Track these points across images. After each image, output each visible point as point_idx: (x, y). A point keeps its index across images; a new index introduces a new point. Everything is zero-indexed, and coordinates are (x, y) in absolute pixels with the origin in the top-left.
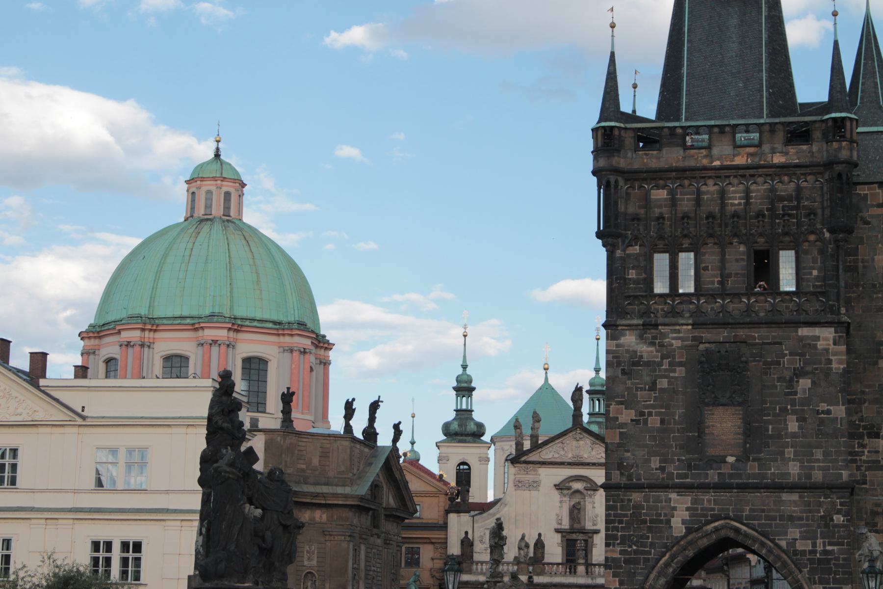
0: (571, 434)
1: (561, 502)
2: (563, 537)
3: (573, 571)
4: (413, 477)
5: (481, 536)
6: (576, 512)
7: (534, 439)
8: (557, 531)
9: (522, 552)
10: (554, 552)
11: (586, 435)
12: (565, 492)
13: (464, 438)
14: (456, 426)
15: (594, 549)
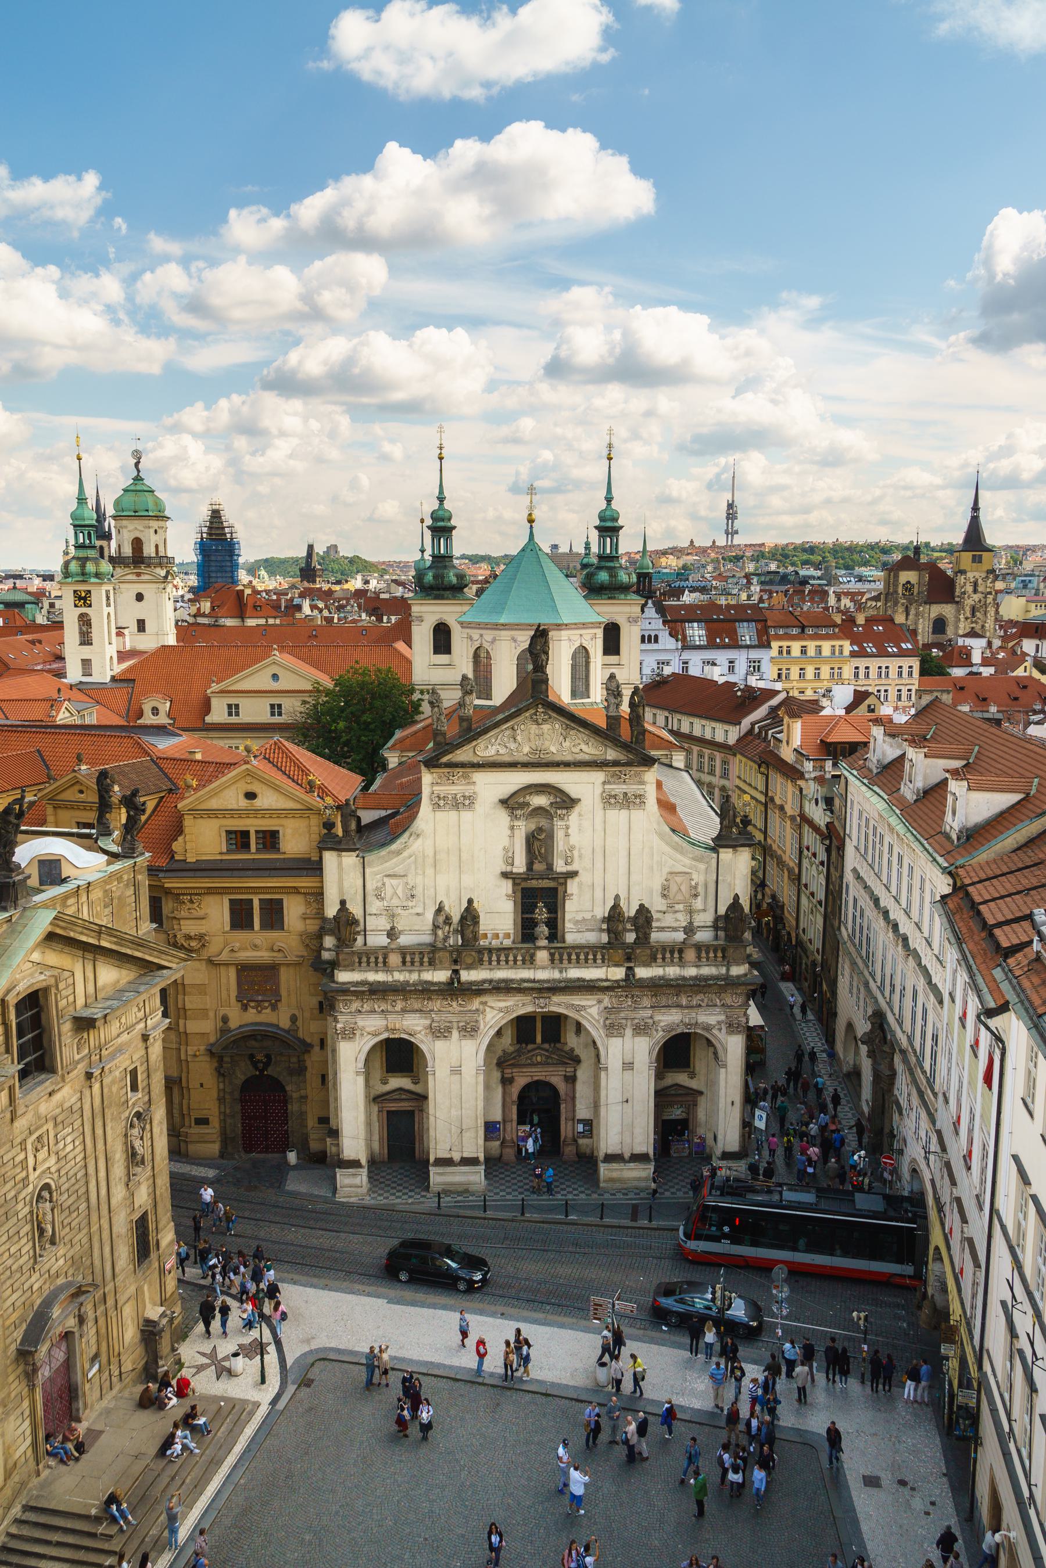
0: (527, 714)
1: (512, 828)
2: (514, 884)
3: (529, 961)
4: (264, 787)
5: (377, 888)
6: (538, 845)
7: (465, 724)
8: (505, 875)
9: (440, 932)
10: (499, 918)
11: (554, 715)
12: (519, 812)
13: (442, 592)
14: (431, 578)
15: (568, 903)
